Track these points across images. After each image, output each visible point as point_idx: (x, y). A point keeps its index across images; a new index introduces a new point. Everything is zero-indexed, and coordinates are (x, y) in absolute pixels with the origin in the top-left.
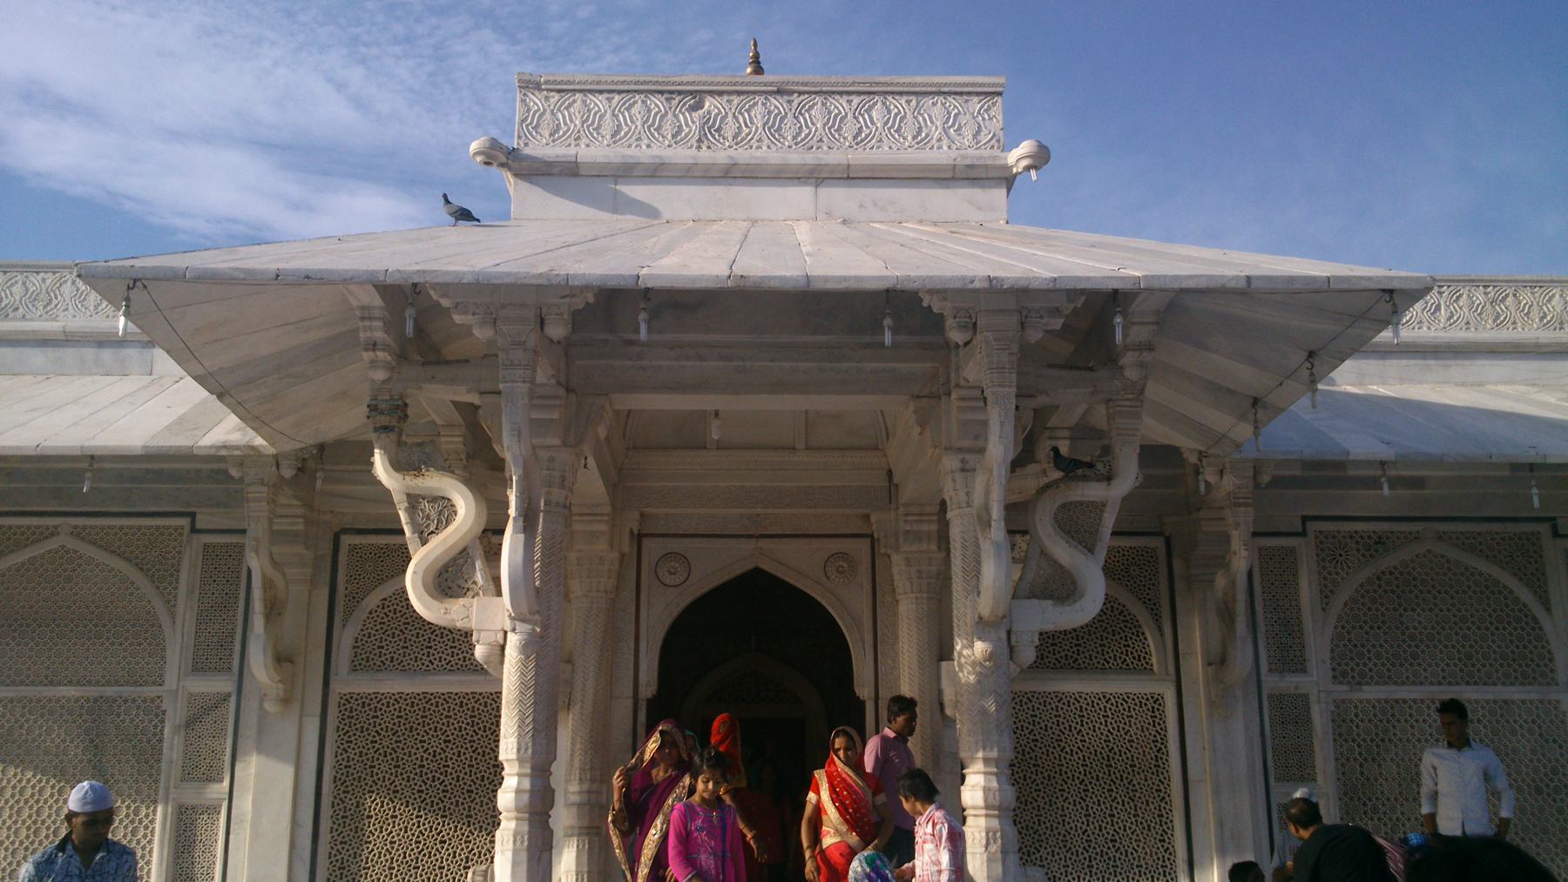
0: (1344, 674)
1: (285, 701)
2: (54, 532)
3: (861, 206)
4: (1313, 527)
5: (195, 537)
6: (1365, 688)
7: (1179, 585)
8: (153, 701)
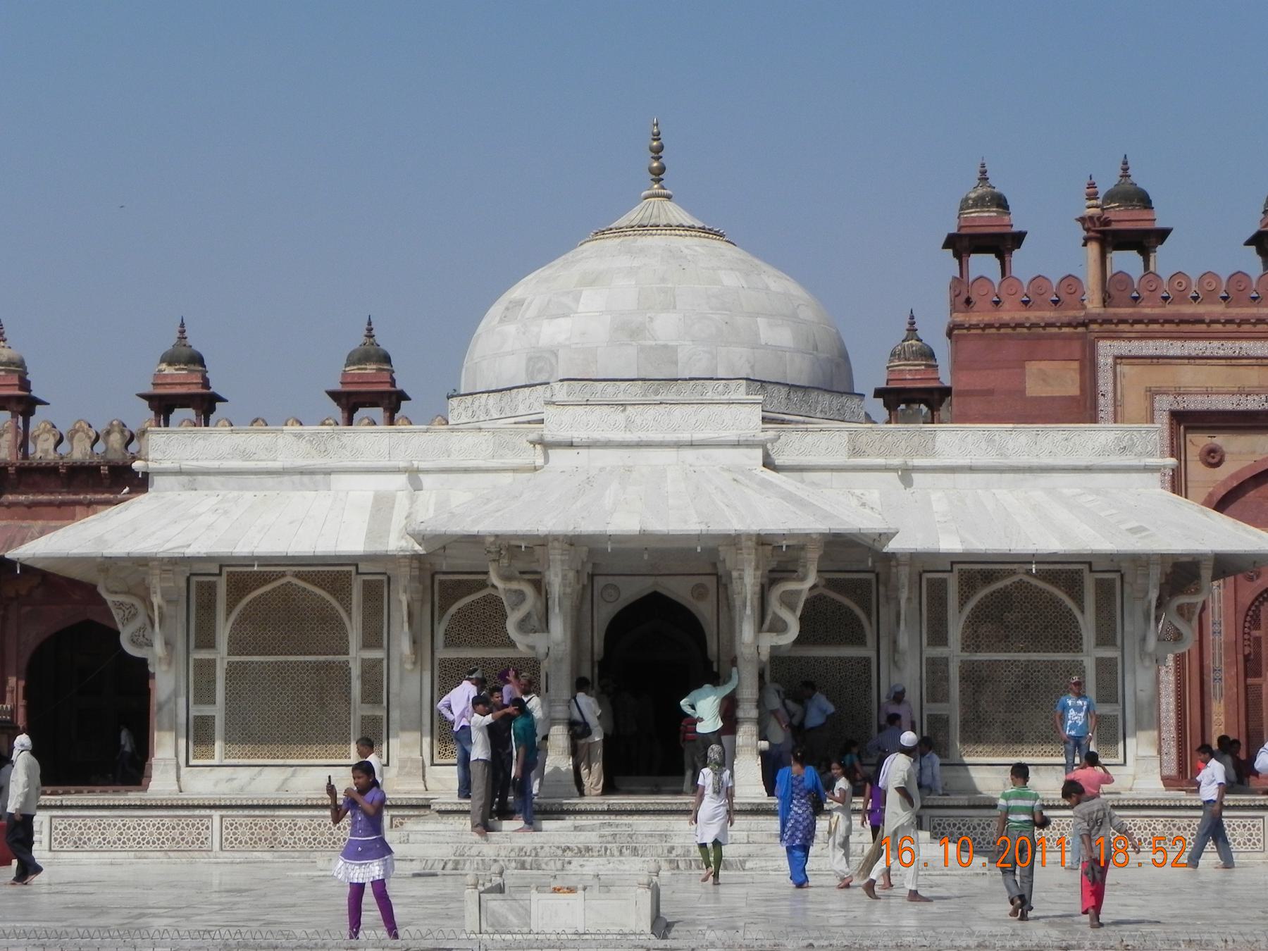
0: (968, 646)
1: (415, 663)
2: (283, 575)
4: (956, 567)
5: (359, 576)
6: (979, 654)
7: (882, 600)
8: (344, 663)
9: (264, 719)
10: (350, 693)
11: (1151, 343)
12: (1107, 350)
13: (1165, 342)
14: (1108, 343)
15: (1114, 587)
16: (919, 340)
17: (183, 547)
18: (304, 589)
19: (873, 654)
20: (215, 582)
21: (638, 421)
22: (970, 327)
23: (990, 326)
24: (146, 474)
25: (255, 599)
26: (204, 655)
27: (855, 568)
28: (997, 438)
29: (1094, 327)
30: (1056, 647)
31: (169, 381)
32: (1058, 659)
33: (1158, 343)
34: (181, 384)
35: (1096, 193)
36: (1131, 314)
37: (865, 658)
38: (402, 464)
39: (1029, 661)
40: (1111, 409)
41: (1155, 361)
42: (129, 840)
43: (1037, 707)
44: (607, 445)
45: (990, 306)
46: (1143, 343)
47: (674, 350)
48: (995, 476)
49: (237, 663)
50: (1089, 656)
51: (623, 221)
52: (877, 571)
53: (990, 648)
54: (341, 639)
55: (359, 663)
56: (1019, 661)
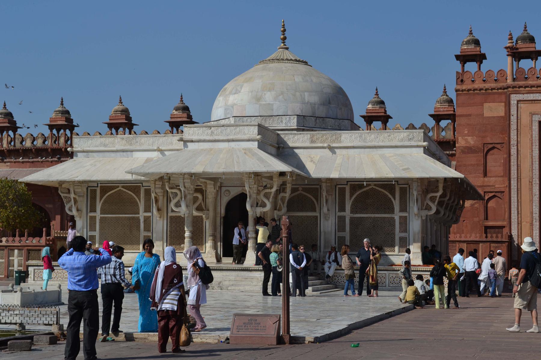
0: (353, 212)
1: (160, 217)
2: (118, 187)
3: (235, 145)
4: (349, 183)
6: (356, 215)
9: (112, 236)
10: (140, 228)
11: (532, 95)
12: (514, 98)
13: (537, 95)
14: (515, 95)
15: (407, 190)
16: (447, 96)
17: (75, 177)
18: (125, 192)
19: (318, 215)
20: (96, 189)
21: (215, 133)
22: (462, 91)
23: (470, 90)
24: (72, 153)
25: (109, 195)
26: (92, 214)
27: (312, 184)
28: (363, 136)
29: (510, 89)
30: (385, 212)
31: (176, 116)
32: (386, 216)
33: (535, 95)
34: (180, 117)
35: (512, 37)
36: (524, 84)
37: (316, 216)
38: (155, 148)
39: (375, 217)
40: (516, 121)
41: (533, 102)
42: (59, 277)
43: (378, 234)
44: (204, 141)
45: (470, 82)
46: (529, 95)
47: (272, 105)
48: (363, 150)
49: (103, 217)
50: (397, 215)
51: (269, 58)
52: (320, 184)
53: (361, 213)
54: (137, 209)
55: (143, 217)
56: (371, 217)
